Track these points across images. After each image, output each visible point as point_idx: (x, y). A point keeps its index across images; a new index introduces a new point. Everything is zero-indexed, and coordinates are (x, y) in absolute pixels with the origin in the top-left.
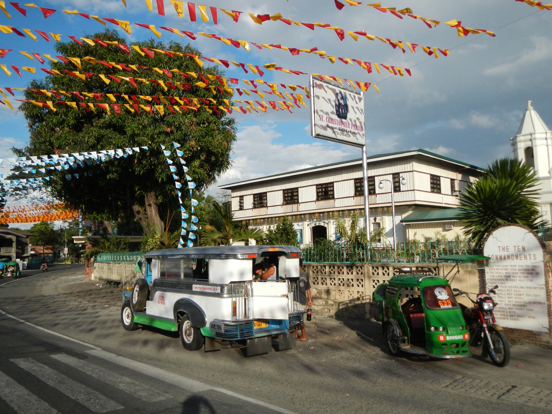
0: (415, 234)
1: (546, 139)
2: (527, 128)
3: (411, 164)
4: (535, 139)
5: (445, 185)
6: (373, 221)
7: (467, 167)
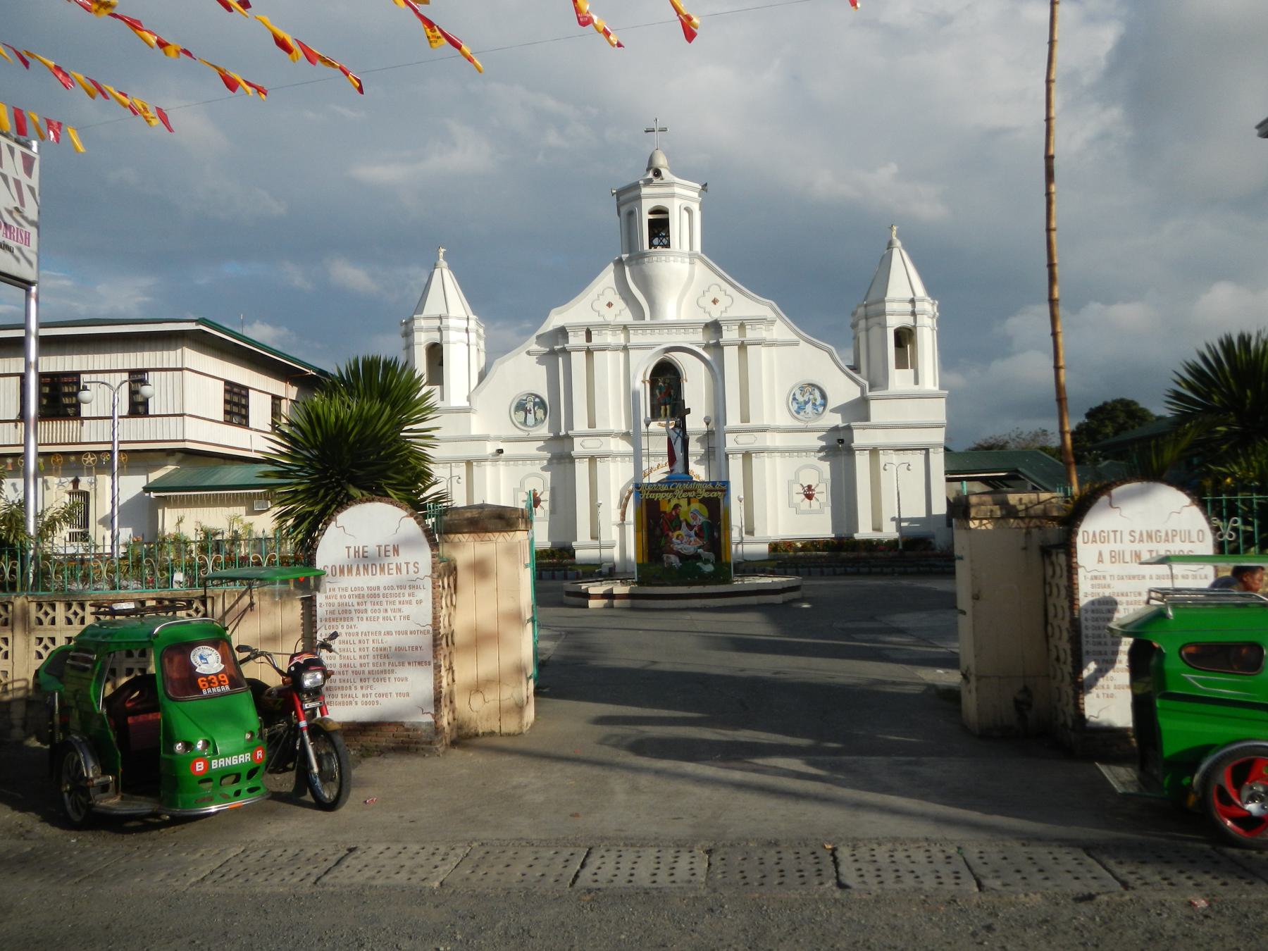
0: (180, 521)
1: (467, 331)
2: (433, 305)
3: (179, 351)
4: (448, 328)
5: (259, 410)
6: (71, 487)
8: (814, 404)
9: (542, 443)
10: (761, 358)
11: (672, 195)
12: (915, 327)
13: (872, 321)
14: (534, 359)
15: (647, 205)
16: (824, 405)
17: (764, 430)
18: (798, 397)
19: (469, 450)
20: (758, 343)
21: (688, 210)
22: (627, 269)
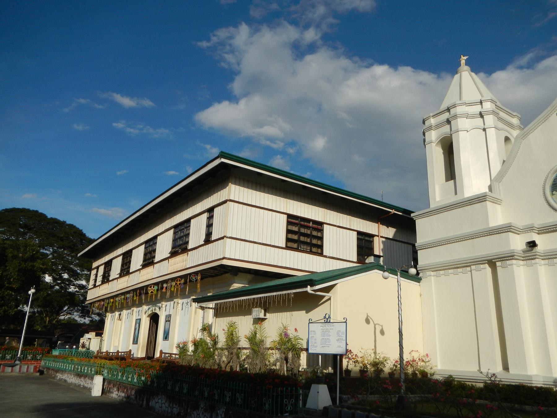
1: (481, 115)
7: (393, 211)
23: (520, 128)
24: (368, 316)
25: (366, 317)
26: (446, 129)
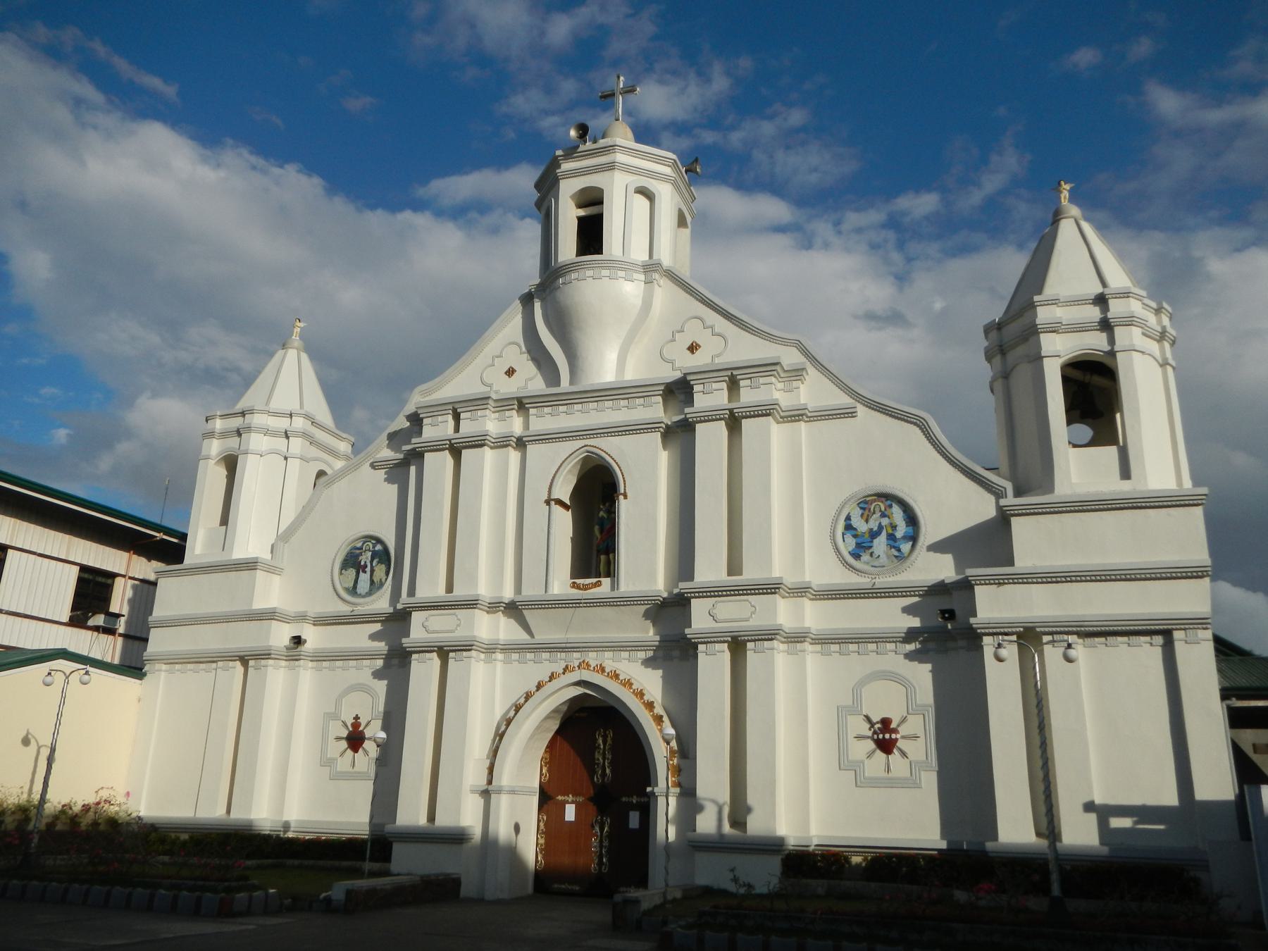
7: (159, 536)
8: (891, 537)
9: (378, 627)
10: (771, 442)
11: (611, 167)
12: (1112, 354)
13: (1012, 356)
14: (381, 474)
15: (568, 189)
16: (913, 538)
17: (771, 589)
18: (858, 522)
19: (243, 637)
20: (764, 411)
21: (644, 192)
22: (537, 305)
23: (347, 458)
24: (28, 733)
25: (24, 734)
26: (233, 442)
